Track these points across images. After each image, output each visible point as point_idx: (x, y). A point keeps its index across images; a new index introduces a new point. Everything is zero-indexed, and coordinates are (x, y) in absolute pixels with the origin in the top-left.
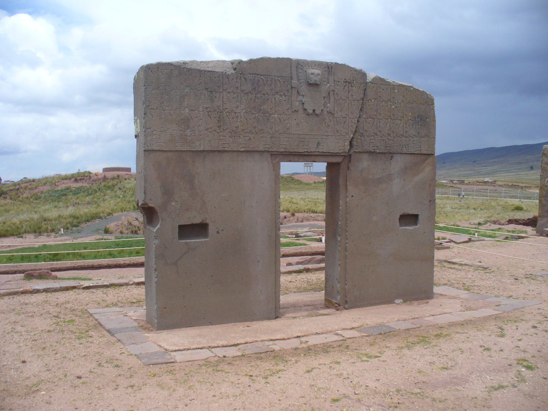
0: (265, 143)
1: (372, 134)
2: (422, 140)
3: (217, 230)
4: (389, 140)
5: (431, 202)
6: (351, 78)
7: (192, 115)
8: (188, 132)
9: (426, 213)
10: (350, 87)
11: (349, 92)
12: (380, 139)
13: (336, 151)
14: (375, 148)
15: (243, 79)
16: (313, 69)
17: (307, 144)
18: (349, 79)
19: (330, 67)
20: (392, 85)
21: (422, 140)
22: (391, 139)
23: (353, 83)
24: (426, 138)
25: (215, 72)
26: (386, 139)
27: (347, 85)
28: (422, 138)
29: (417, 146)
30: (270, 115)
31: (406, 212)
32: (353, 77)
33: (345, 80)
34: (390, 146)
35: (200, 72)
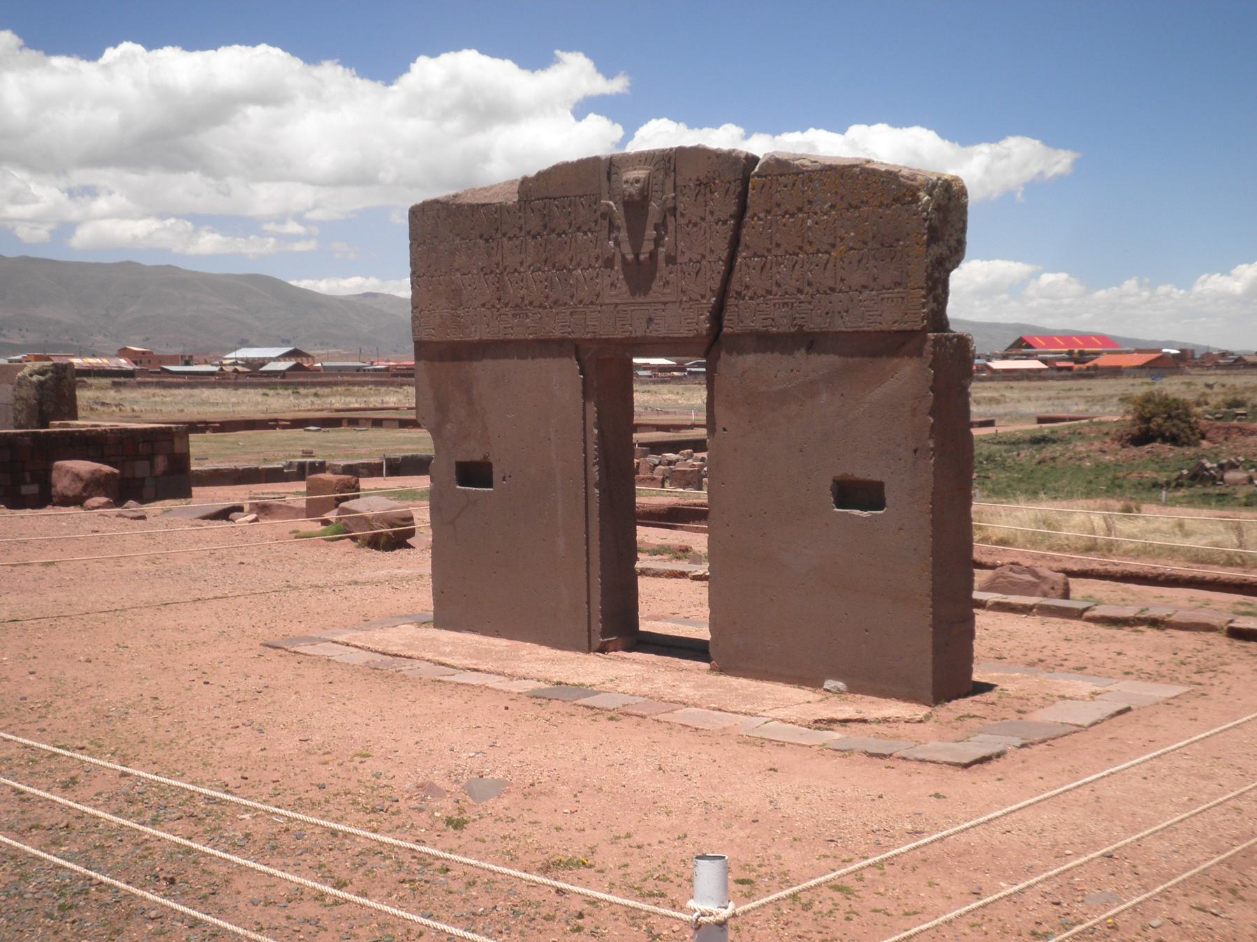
0: (564, 324)
1: (760, 292)
2: (883, 296)
3: (503, 475)
4: (800, 303)
5: (918, 454)
6: (709, 175)
7: (464, 281)
8: (460, 312)
9: (903, 480)
10: (709, 195)
11: (706, 206)
12: (780, 301)
13: (684, 332)
14: (769, 322)
15: (529, 211)
16: (635, 169)
17: (629, 322)
18: (706, 177)
19: (666, 159)
20: (807, 171)
21: (883, 296)
22: (805, 300)
23: (714, 183)
24: (896, 290)
25: (490, 204)
26: (794, 300)
27: (703, 192)
28: (884, 291)
29: (871, 313)
30: (570, 271)
31: (850, 474)
32: (714, 172)
33: (698, 180)
34: (803, 315)
35: (475, 208)
